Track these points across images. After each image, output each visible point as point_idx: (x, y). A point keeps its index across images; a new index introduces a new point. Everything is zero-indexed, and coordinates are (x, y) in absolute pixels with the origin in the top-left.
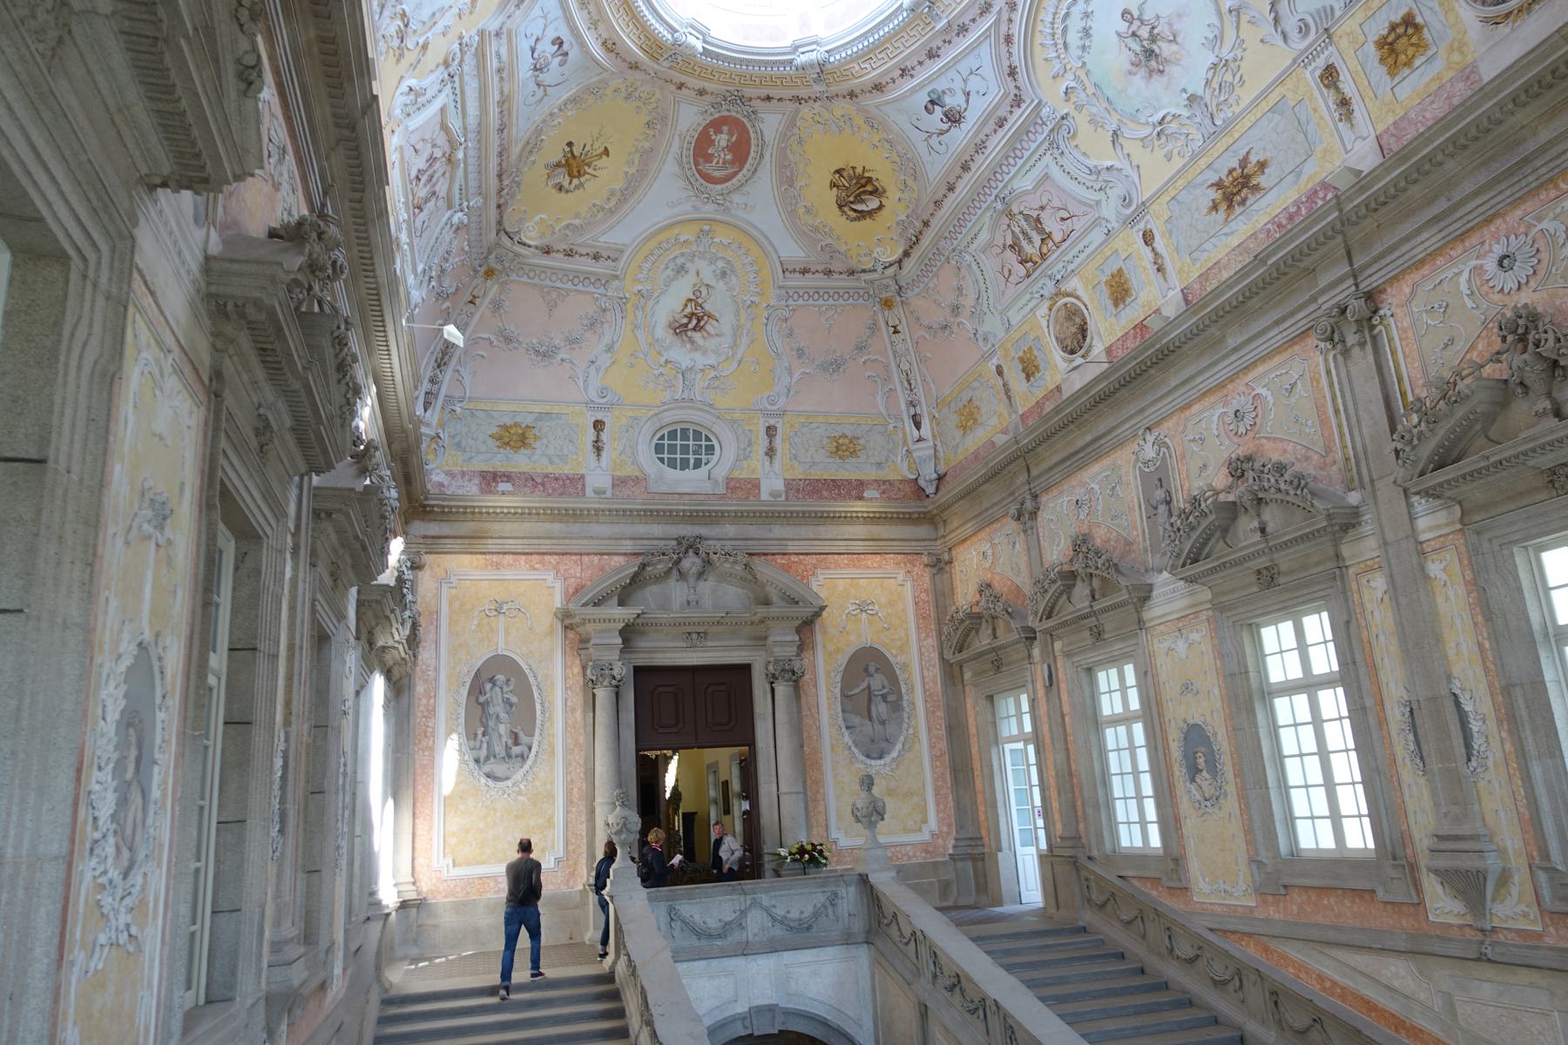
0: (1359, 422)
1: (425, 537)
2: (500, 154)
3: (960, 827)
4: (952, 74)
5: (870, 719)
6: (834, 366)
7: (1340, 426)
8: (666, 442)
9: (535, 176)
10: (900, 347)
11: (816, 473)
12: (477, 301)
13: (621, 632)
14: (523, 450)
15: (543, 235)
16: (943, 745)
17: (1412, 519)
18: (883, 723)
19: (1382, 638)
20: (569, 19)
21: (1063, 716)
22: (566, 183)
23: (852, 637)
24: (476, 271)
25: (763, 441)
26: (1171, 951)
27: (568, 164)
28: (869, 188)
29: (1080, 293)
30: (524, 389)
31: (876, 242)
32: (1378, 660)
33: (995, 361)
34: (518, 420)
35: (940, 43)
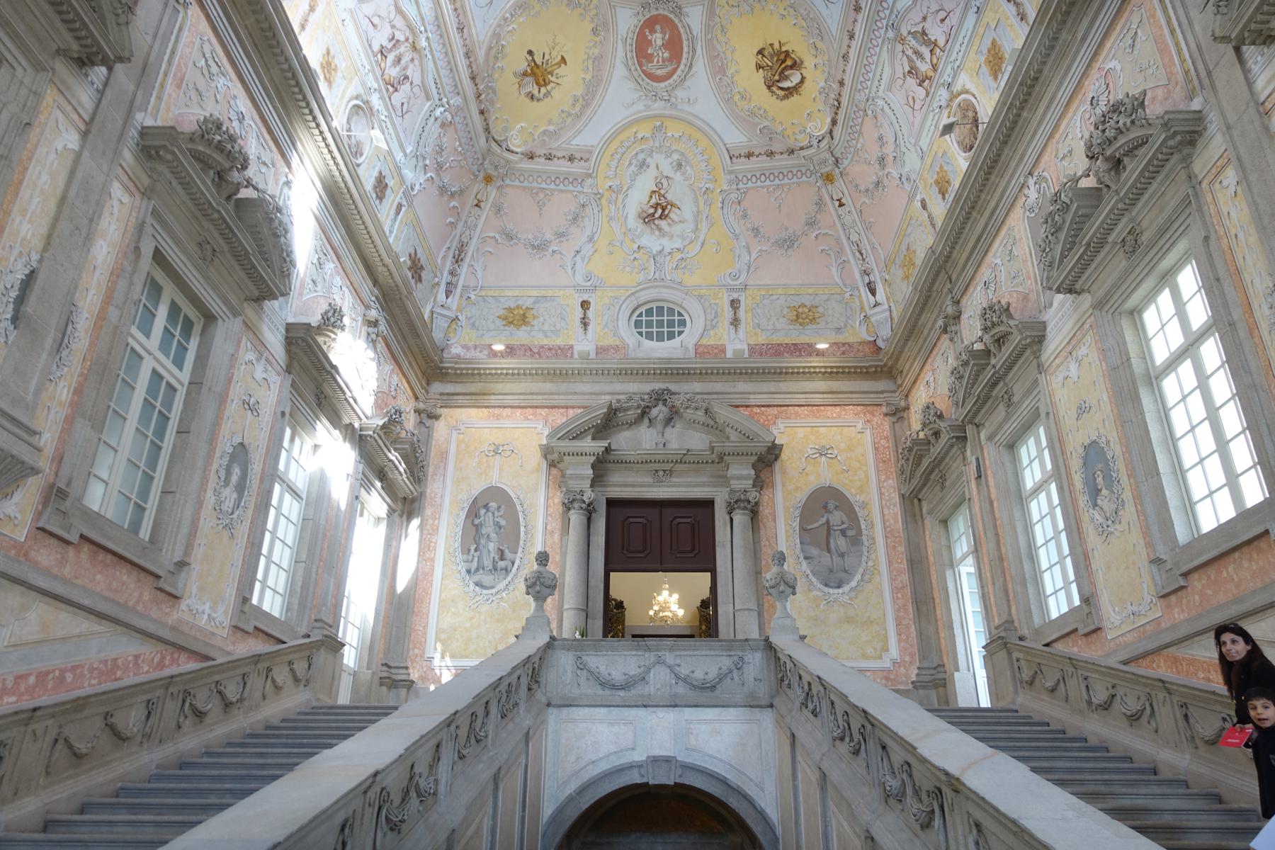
0: (1190, 23)
1: (442, 394)
2: (467, 55)
3: (924, 656)
5: (829, 551)
6: (788, 243)
7: (1177, 44)
8: (644, 318)
9: (506, 83)
10: (848, 220)
11: (778, 339)
12: (482, 205)
13: (593, 466)
14: (524, 328)
15: (525, 142)
16: (905, 578)
17: (1250, 84)
18: (842, 555)
19: (1241, 236)
21: (991, 503)
22: (535, 92)
23: (812, 478)
24: (476, 176)
25: (728, 313)
26: (1090, 703)
27: (533, 74)
28: (789, 62)
29: (968, 87)
30: (524, 278)
31: (805, 117)
32: (1240, 263)
33: (919, 197)
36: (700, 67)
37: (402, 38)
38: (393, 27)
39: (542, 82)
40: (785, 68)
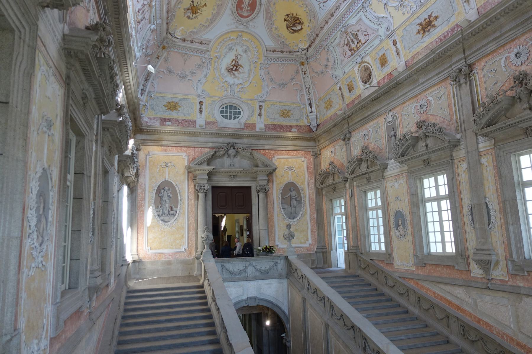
0: (462, 110)
1: (141, 140)
2: (168, 4)
3: (319, 242)
5: (291, 206)
6: (283, 85)
7: (456, 111)
9: (180, 12)
10: (306, 79)
11: (276, 122)
12: (159, 58)
13: (208, 174)
14: (175, 111)
16: (315, 215)
17: (478, 144)
18: (295, 207)
19: (464, 184)
21: (355, 207)
22: (191, 16)
23: (286, 179)
25: (257, 111)
26: (386, 283)
27: (192, 9)
28: (298, 22)
29: (370, 62)
30: (175, 90)
31: (299, 41)
32: (462, 191)
33: (339, 85)
34: (173, 100)
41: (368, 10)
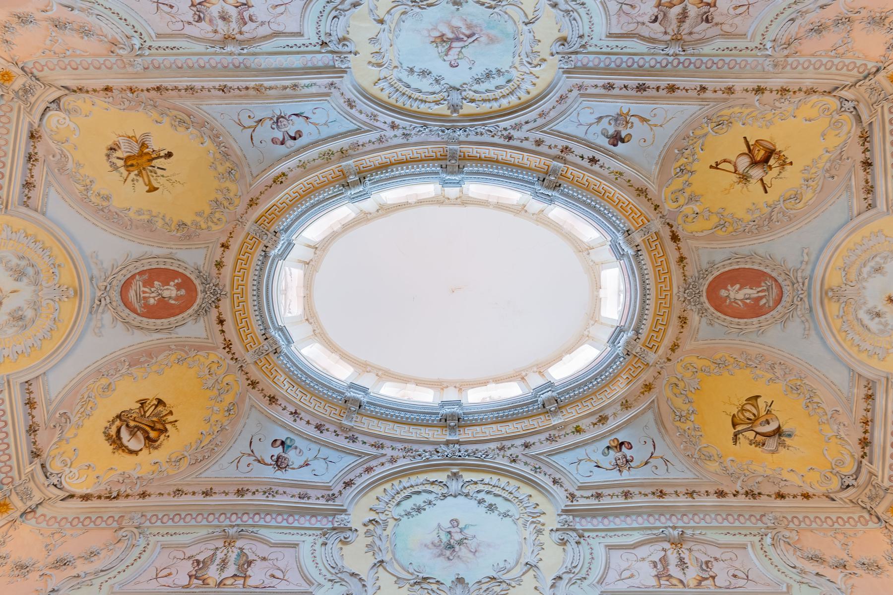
2: (191, 89)
4: (315, 447)
20: (315, 144)
22: (119, 154)
27: (141, 154)
28: (153, 434)
35: (332, 428)
36: (138, 339)
37: (245, 29)
38: (263, 23)
39: (129, 163)
40: (147, 432)
41: (329, 546)
